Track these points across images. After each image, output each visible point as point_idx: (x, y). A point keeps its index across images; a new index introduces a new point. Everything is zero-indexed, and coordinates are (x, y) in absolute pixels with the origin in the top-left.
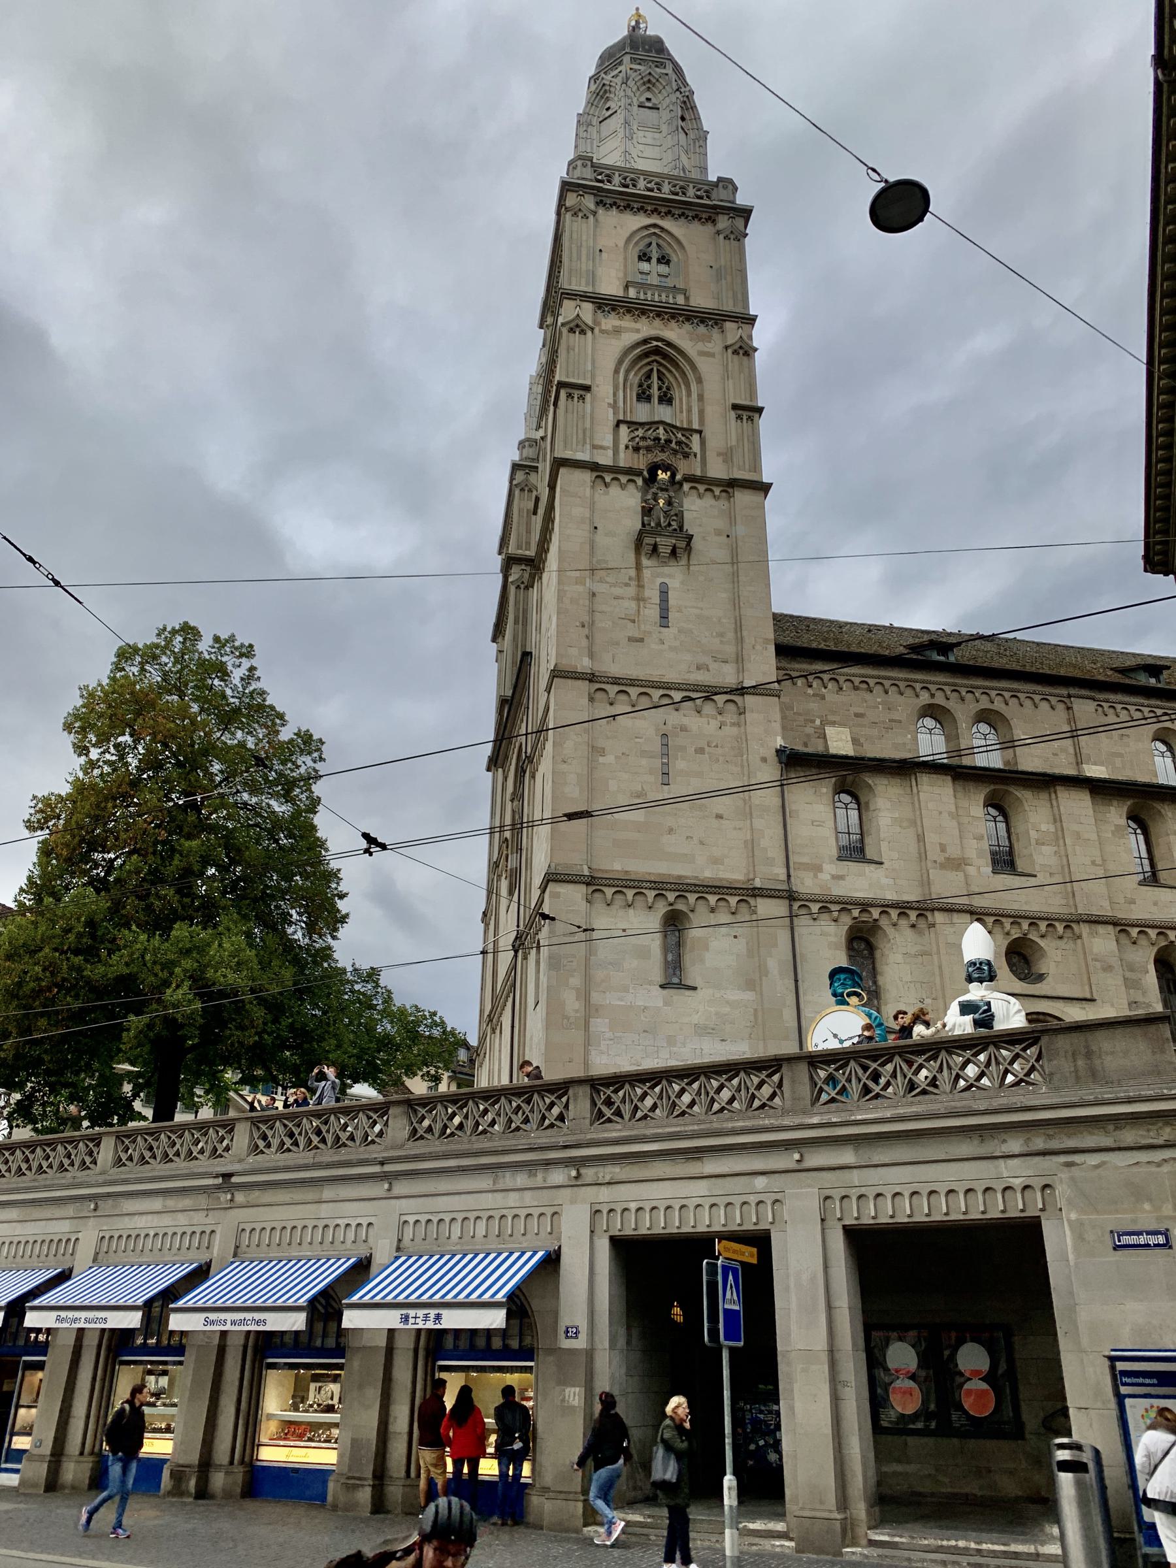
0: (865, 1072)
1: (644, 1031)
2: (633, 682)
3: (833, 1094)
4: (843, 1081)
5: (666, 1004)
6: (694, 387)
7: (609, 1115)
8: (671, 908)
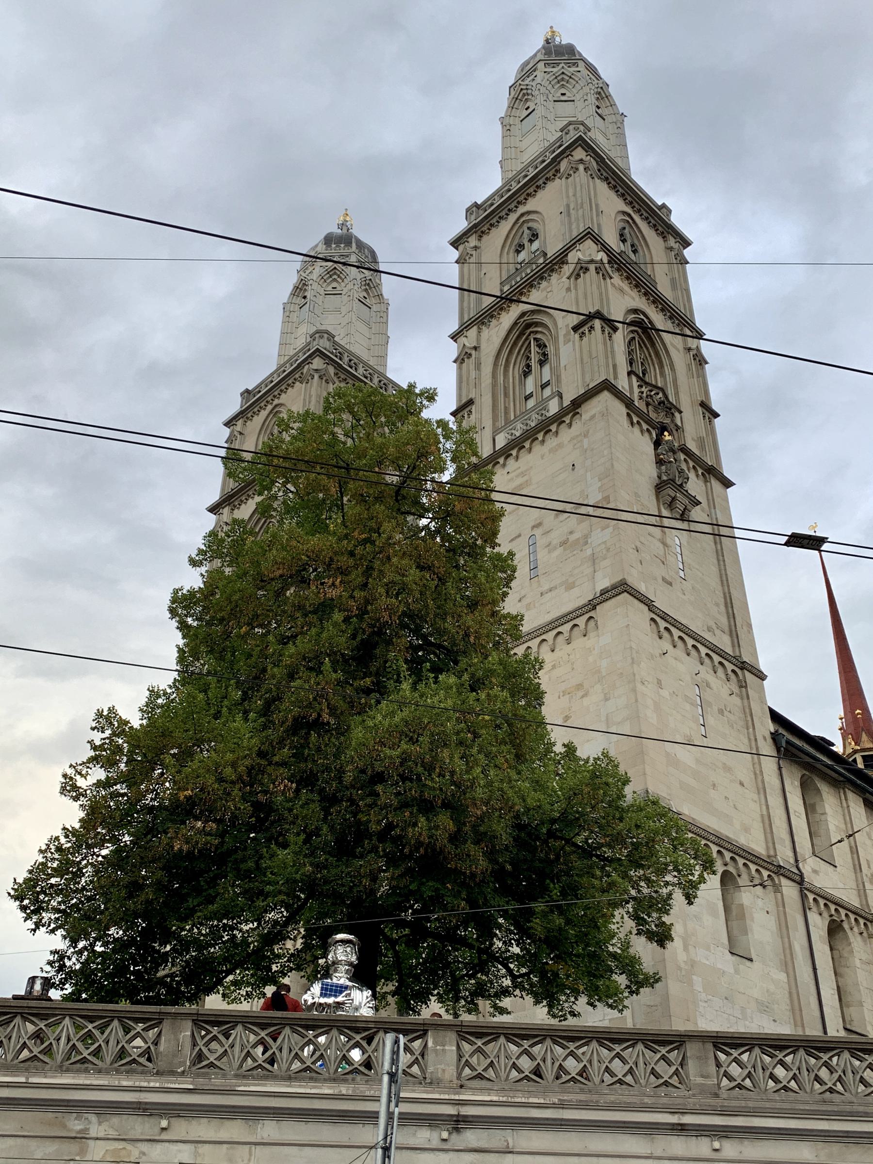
0: (77, 1033)
1: (726, 998)
2: (676, 623)
3: (36, 1051)
4: (274, 1049)
5: (737, 971)
6: (667, 370)
7: (212, 1059)
8: (725, 868)
